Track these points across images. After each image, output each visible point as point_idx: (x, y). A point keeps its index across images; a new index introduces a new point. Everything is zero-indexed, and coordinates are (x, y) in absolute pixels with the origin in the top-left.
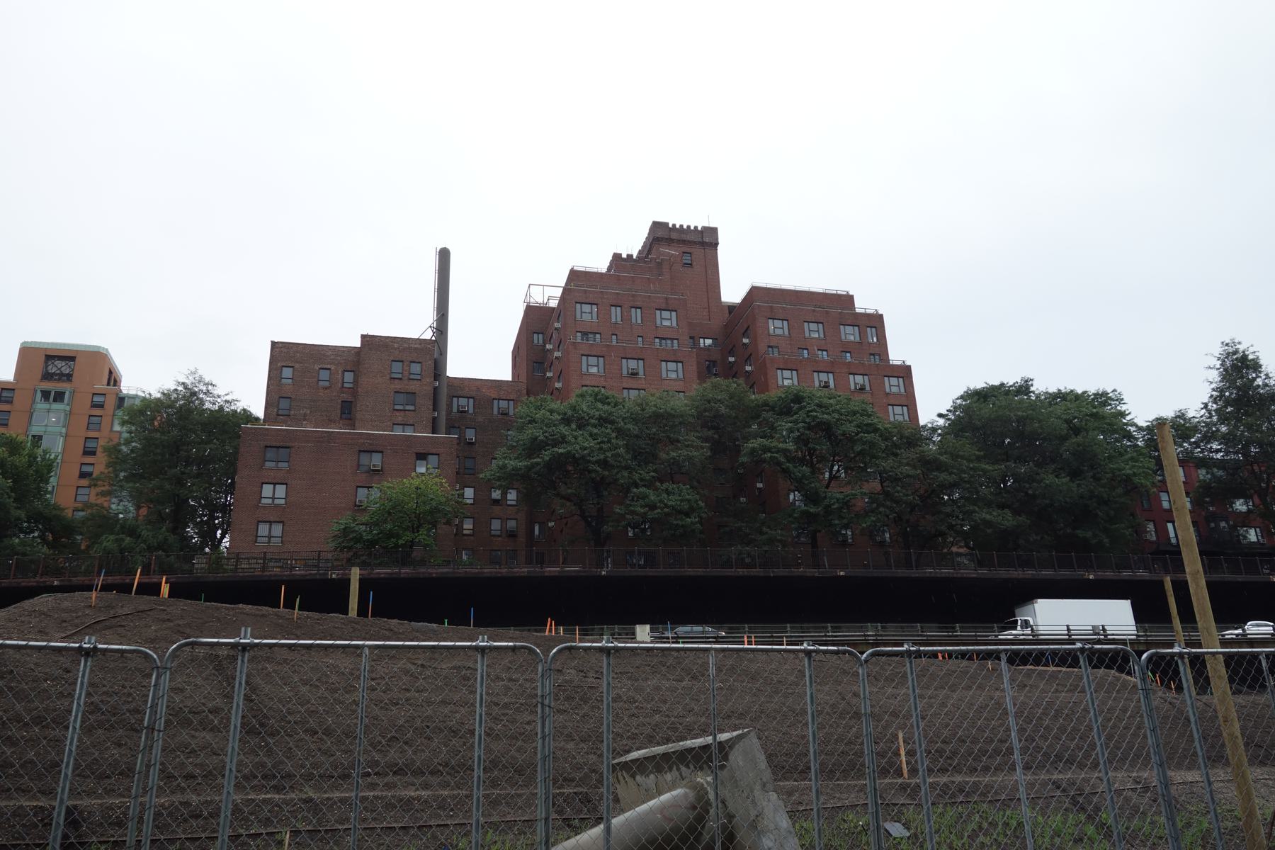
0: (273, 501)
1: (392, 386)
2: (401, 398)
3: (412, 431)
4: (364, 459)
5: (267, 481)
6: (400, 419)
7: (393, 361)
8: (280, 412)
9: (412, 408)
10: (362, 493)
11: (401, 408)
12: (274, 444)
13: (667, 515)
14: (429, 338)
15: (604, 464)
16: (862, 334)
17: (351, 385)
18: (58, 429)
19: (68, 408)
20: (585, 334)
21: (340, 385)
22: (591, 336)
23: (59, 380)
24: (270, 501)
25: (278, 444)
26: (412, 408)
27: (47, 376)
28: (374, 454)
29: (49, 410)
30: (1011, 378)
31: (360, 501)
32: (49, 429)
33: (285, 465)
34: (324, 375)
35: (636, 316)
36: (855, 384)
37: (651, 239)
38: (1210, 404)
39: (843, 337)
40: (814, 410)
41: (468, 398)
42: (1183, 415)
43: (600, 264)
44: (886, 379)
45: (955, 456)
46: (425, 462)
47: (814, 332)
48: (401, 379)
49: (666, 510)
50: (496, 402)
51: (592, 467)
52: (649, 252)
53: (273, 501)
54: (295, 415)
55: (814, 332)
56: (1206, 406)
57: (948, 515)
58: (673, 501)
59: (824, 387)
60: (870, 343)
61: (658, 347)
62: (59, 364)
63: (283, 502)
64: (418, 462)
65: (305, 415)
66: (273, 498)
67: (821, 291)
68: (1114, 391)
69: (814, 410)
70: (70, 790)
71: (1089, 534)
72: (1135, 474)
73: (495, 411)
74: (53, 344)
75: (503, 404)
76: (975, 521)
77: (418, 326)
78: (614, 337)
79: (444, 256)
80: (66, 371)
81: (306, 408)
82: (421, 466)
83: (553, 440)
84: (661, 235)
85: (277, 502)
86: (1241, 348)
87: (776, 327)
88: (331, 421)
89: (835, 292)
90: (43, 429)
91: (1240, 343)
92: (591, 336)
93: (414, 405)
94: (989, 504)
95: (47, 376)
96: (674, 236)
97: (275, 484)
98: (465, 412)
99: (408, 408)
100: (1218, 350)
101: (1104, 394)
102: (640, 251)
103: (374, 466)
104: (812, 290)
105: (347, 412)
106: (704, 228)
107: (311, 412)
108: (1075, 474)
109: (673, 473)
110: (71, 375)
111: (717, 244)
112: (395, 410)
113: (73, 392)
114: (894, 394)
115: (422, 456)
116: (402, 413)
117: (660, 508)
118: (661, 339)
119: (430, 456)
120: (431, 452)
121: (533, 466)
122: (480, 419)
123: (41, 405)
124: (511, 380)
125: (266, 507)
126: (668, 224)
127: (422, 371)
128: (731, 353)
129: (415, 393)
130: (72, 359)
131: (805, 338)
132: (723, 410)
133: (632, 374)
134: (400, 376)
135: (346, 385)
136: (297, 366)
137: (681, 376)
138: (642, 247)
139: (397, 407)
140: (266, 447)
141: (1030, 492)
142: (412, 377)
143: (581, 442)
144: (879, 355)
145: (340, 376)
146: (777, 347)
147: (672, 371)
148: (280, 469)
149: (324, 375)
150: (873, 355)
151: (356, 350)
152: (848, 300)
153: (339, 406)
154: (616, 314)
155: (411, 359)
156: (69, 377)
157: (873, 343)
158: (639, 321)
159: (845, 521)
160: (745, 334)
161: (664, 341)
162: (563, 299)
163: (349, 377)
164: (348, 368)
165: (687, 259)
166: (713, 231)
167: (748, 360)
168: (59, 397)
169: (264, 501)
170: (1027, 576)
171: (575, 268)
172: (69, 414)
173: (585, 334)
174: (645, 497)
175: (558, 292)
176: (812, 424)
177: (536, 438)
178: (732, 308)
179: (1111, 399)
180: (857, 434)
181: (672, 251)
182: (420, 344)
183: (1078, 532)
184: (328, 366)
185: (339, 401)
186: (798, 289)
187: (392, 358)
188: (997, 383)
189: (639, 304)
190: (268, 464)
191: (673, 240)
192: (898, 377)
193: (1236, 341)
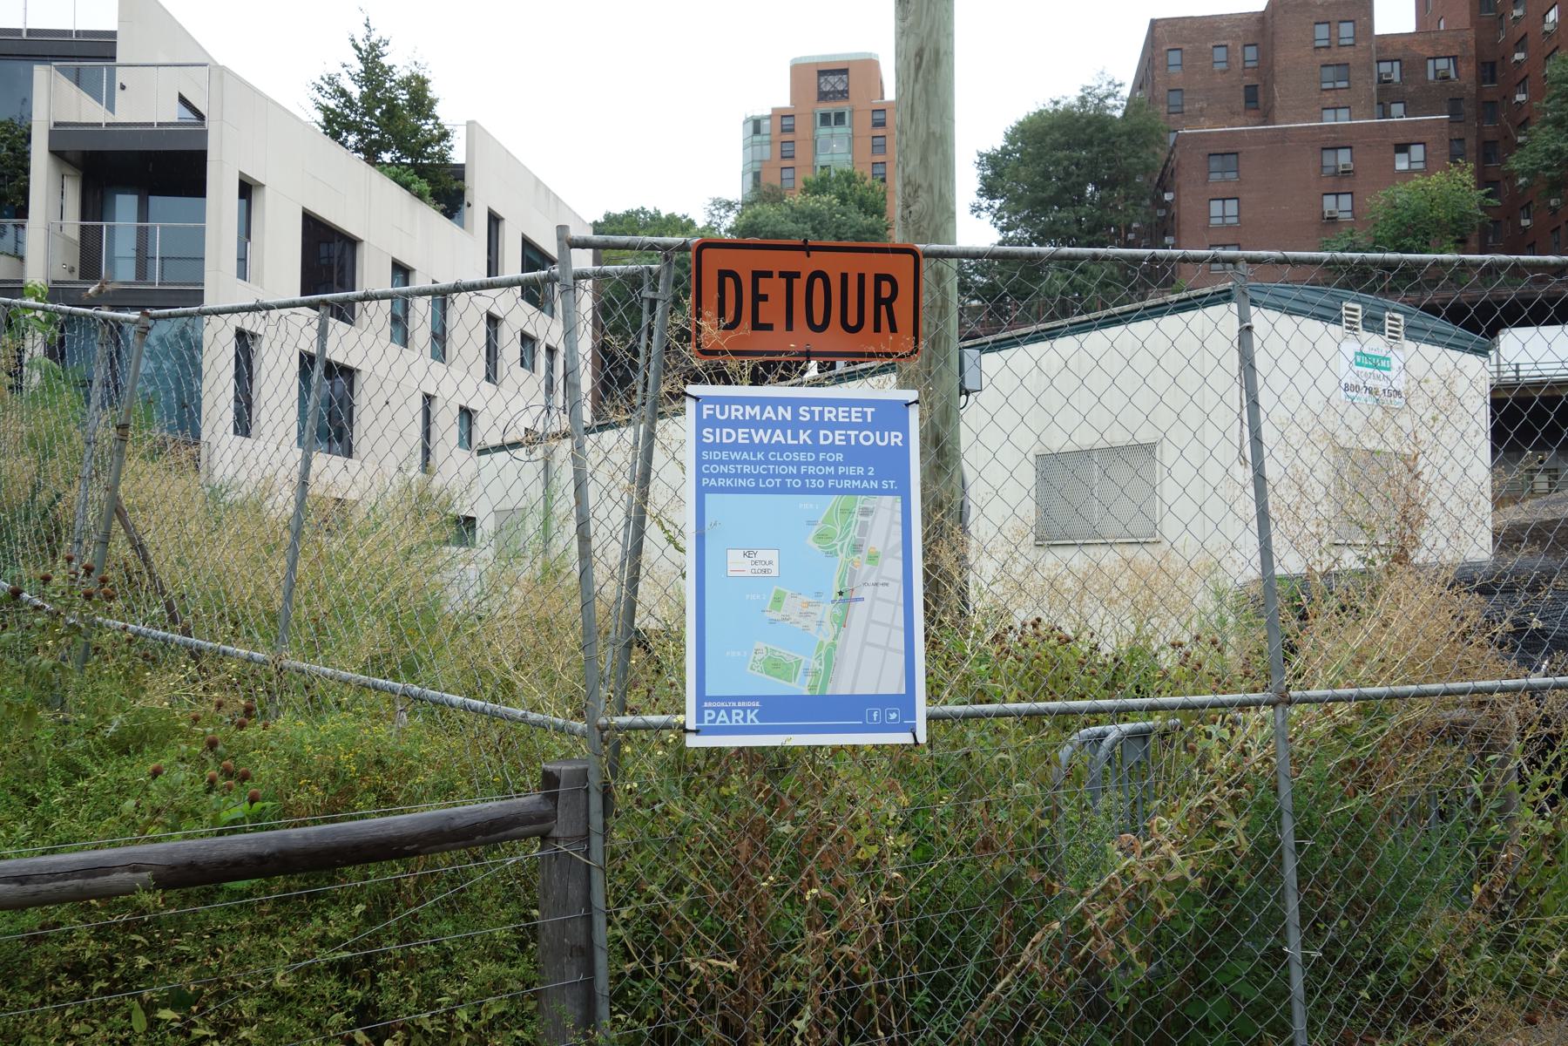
1: (1318, 58)
2: (1329, 73)
4: (1328, 159)
6: (1330, 102)
8: (1172, 110)
9: (1345, 84)
10: (1329, 202)
11: (1330, 86)
17: (1255, 64)
18: (843, 157)
19: (850, 131)
21: (1241, 66)
23: (834, 98)
25: (1223, 151)
26: (1345, 84)
27: (823, 96)
28: (1340, 151)
29: (832, 136)
31: (1330, 212)
32: (836, 157)
33: (1233, 175)
34: (1220, 54)
41: (1392, 61)
46: (1406, 155)
48: (1328, 47)
50: (1430, 63)
54: (1189, 111)
62: (832, 79)
63: (1235, 220)
64: (1398, 156)
65: (1201, 110)
73: (1431, 76)
74: (823, 56)
80: (841, 87)
82: (1402, 161)
85: (1228, 220)
88: (1233, 113)
90: (829, 157)
93: (1348, 80)
95: (823, 96)
97: (1224, 200)
98: (1389, 81)
99: (1339, 85)
103: (1344, 166)
105: (1256, 99)
110: (847, 92)
113: (852, 112)
115: (1403, 148)
119: (1413, 147)
122: (1410, 89)
123: (824, 131)
124: (1379, 29)
125: (1218, 228)
130: (845, 71)
134: (1326, 43)
135: (1248, 65)
136: (1186, 47)
139: (1325, 86)
142: (1342, 42)
145: (1240, 54)
148: (1227, 181)
149: (1220, 54)
153: (1242, 94)
155: (1339, 18)
156: (843, 94)
163: (1251, 53)
168: (840, 118)
169: (1213, 221)
172: (852, 138)
185: (1242, 87)
190: (1213, 176)
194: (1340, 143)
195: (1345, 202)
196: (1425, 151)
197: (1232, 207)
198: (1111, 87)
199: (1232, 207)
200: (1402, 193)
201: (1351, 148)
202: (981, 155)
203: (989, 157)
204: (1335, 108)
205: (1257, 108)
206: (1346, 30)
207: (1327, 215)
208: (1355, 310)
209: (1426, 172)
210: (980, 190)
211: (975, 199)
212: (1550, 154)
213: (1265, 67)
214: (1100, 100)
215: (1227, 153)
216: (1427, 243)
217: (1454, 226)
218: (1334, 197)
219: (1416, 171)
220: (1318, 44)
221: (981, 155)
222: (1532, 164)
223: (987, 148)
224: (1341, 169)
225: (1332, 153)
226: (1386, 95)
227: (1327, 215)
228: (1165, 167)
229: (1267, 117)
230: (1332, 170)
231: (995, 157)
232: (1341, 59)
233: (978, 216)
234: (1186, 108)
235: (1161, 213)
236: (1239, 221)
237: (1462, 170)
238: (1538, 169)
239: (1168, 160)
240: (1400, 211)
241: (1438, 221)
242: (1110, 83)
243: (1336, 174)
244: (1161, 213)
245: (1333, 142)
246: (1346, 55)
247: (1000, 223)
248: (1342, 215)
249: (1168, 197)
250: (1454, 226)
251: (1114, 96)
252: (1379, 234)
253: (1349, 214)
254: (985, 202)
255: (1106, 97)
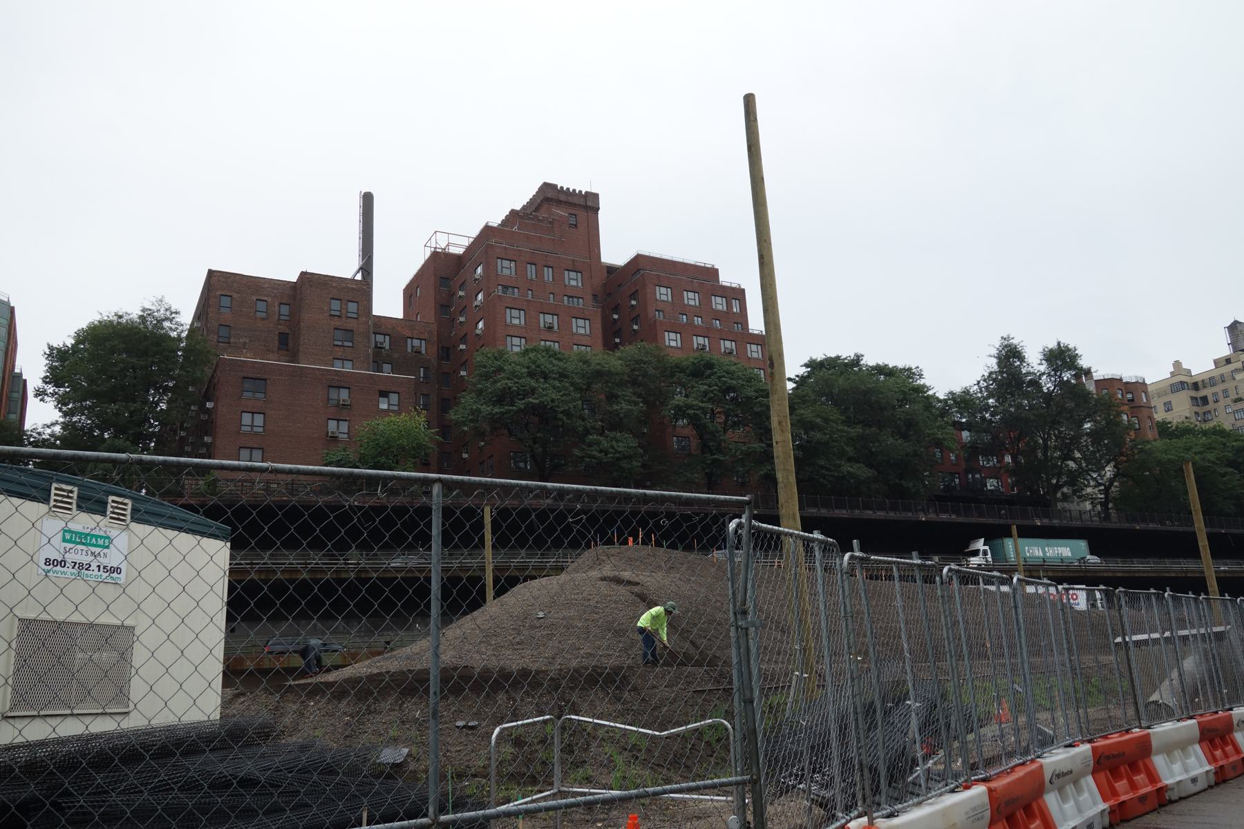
0: (252, 429)
1: (332, 322)
2: (339, 334)
3: (351, 366)
4: (333, 394)
5: (246, 410)
6: (339, 354)
7: (332, 299)
8: (220, 340)
9: (350, 344)
10: (332, 425)
11: (340, 343)
12: (251, 376)
13: (618, 459)
14: (349, 276)
15: (567, 413)
16: (729, 305)
20: (505, 287)
22: (510, 290)
24: (249, 429)
26: (350, 344)
30: (847, 353)
31: (333, 433)
33: (261, 395)
34: (261, 306)
35: (548, 274)
36: (725, 348)
37: (541, 198)
38: (982, 382)
39: (714, 307)
40: (724, 376)
41: (385, 335)
42: (968, 391)
43: (496, 220)
44: (748, 345)
45: (826, 420)
47: (691, 299)
48: (339, 316)
49: (617, 455)
50: (409, 340)
51: (560, 416)
52: (537, 209)
53: (252, 429)
55: (691, 299)
56: (979, 382)
57: (822, 467)
58: (621, 447)
59: (702, 349)
60: (734, 313)
61: (552, 301)
63: (261, 430)
65: (244, 344)
66: (252, 426)
67: (692, 263)
68: (918, 367)
69: (724, 376)
70: (1052, 650)
71: (911, 484)
72: (944, 439)
73: (409, 350)
75: (416, 343)
76: (843, 473)
77: (345, 267)
78: (530, 292)
79: (368, 200)
81: (245, 337)
82: (384, 403)
83: (523, 390)
84: (549, 196)
85: (256, 429)
86: (1014, 342)
87: (663, 294)
88: (269, 351)
89: (703, 265)
91: (1013, 338)
92: (510, 290)
93: (352, 342)
94: (850, 460)
96: (562, 198)
97: (253, 413)
99: (346, 344)
100: (998, 343)
101: (910, 369)
102: (524, 206)
103: (344, 401)
104: (663, 257)
105: (287, 343)
106: (586, 192)
107: (251, 341)
108: (905, 437)
109: (616, 424)
111: (598, 209)
112: (334, 345)
114: (754, 358)
115: (384, 394)
116: (341, 349)
117: (611, 453)
118: (569, 297)
120: (393, 390)
121: (508, 412)
122: (396, 356)
125: (245, 434)
126: (557, 186)
127: (358, 310)
128: (616, 309)
129: (352, 331)
131: (657, 300)
132: (651, 371)
133: (549, 328)
134: (338, 313)
135: (282, 317)
136: (235, 295)
137: (588, 332)
138: (531, 199)
139: (336, 343)
140: (244, 378)
141: (873, 450)
142: (349, 315)
143: (548, 393)
144: (741, 324)
146: (663, 311)
147: (581, 327)
149: (261, 306)
150: (737, 323)
151: (293, 285)
152: (713, 273)
153: (277, 338)
154: (531, 271)
155: (349, 298)
157: (736, 313)
158: (551, 279)
159: (747, 468)
160: (633, 296)
161: (571, 299)
162: (469, 249)
163: (285, 310)
164: (284, 301)
165: (572, 221)
166: (596, 196)
167: (635, 320)
170: (865, 517)
171: (490, 224)
173: (505, 287)
174: (598, 443)
175: (466, 242)
176: (723, 387)
177: (510, 388)
178: (611, 269)
179: (914, 374)
180: (756, 398)
181: (560, 212)
182: (356, 285)
183: (903, 482)
184: (266, 298)
185: (277, 332)
186: (674, 259)
187: (331, 296)
188: (833, 355)
189: (550, 264)
190: (245, 394)
191: (561, 201)
192: (757, 345)
193: (1011, 336)
194: (343, 384)
195: (344, 427)
196: (399, 399)
197: (259, 420)
198: (168, 313)
199: (259, 420)
200: (382, 424)
201: (349, 388)
202: (51, 348)
203: (59, 350)
204: (343, 360)
205: (288, 350)
206: (352, 307)
207: (330, 434)
208: (125, 504)
209: (398, 413)
210: (46, 377)
211: (40, 384)
212: (473, 412)
213: (294, 320)
214: (158, 321)
215: (258, 379)
216: (397, 463)
217: (413, 452)
218: (336, 422)
219: (393, 411)
220: (332, 313)
221: (51, 348)
222: (463, 417)
223: (57, 343)
224: (341, 402)
225: (336, 390)
226: (379, 357)
227: (330, 434)
228: (210, 381)
229: (294, 357)
230: (336, 402)
231: (66, 352)
232: (349, 326)
233: (41, 400)
234: (232, 340)
235: (204, 417)
236: (264, 431)
237: (419, 414)
238: (466, 421)
239: (212, 377)
240: (378, 437)
241: (403, 448)
242: (167, 310)
243: (338, 406)
244: (204, 417)
245: (338, 382)
246: (351, 324)
247: (64, 408)
248: (341, 436)
249: (209, 405)
250: (413, 452)
251: (171, 320)
252: (363, 451)
253: (346, 436)
254: (50, 389)
255: (163, 320)
